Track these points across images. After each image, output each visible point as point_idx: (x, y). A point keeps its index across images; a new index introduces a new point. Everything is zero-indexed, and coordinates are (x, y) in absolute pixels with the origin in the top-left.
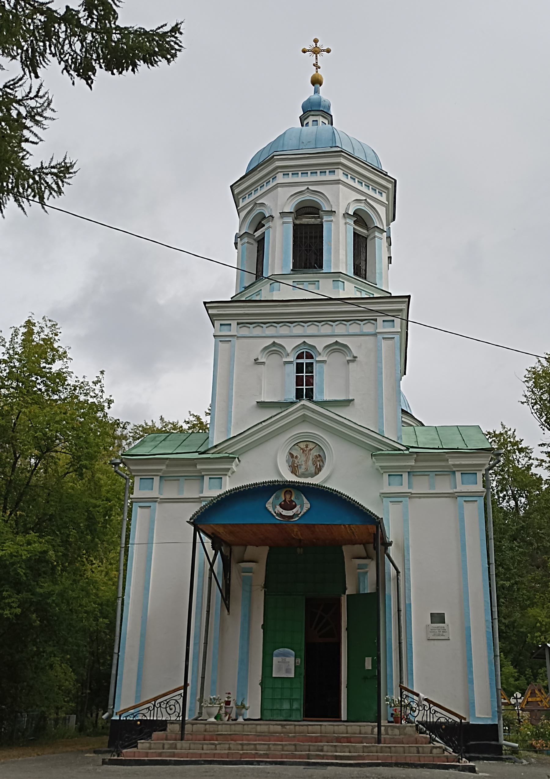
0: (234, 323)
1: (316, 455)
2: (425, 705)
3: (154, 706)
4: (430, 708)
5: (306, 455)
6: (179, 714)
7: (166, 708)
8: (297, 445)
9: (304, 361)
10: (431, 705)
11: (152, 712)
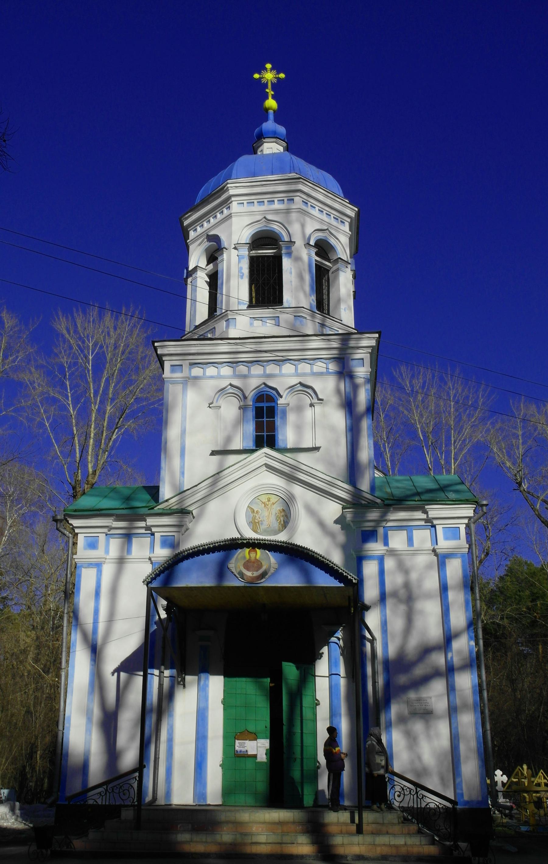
0: (186, 364)
1: (279, 510)
2: (411, 789)
3: (106, 790)
4: (417, 793)
5: (268, 510)
6: (134, 800)
7: (119, 793)
8: (258, 499)
9: (265, 405)
10: (418, 789)
11: (104, 797)
